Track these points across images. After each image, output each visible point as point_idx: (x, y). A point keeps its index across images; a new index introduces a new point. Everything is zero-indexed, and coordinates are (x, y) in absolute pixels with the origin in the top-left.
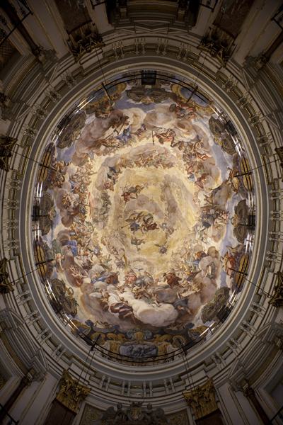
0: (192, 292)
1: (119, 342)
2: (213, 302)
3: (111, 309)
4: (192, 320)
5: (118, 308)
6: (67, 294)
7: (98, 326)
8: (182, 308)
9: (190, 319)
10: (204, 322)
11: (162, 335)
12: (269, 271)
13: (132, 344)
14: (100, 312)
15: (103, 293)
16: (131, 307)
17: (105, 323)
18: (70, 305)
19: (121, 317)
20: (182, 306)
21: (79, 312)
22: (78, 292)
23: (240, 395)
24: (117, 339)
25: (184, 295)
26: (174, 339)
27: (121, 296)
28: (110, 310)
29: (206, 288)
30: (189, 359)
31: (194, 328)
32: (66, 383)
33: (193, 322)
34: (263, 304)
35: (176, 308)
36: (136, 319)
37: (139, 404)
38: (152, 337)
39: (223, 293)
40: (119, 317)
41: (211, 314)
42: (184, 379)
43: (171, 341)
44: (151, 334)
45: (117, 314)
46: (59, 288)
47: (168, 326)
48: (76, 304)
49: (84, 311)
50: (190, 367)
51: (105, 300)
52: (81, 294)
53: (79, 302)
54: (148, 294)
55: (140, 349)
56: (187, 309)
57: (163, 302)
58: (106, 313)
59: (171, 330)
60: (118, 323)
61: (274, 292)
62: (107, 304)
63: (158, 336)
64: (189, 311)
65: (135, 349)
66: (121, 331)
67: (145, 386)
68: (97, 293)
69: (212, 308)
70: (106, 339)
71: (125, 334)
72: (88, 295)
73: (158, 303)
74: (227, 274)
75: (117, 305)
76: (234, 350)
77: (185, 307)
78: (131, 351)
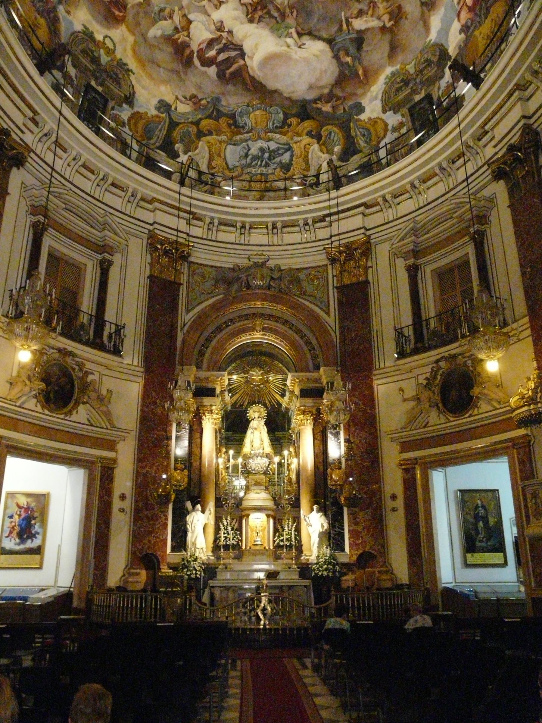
0: (374, 23)
1: (224, 138)
2: (411, 68)
3: (200, 58)
4: (364, 94)
5: (212, 53)
6: (104, 59)
7: (183, 108)
8: (349, 59)
9: (359, 91)
10: (384, 111)
11: (303, 120)
12: (520, 99)
13: (246, 141)
14: (178, 72)
15: (177, 18)
16: (239, 48)
17: (193, 97)
18: (117, 81)
19: (221, 75)
20: (348, 54)
21: (138, 89)
22: (124, 39)
23: (401, 264)
24: (219, 132)
25: (359, 24)
26: (324, 133)
27: (216, 15)
28: (196, 62)
29: (406, 25)
30: (340, 197)
31: (364, 117)
32: (157, 249)
33: (365, 102)
34: (485, 146)
35: (336, 57)
36: (253, 78)
37: (263, 264)
38: (284, 123)
39: (435, 59)
40: (218, 75)
41: (401, 96)
42: (331, 222)
43: (318, 137)
44: (281, 116)
45: (213, 70)
46: (84, 52)
47: (315, 101)
48: (129, 71)
49: (146, 82)
50: (340, 208)
51: (182, 37)
52: (131, 39)
53: (132, 64)
54: (278, 10)
55: (262, 150)
56: (357, 64)
57: (310, 34)
58: (189, 71)
59: (321, 109)
60: (217, 91)
61: (505, 149)
62: (186, 45)
63: (294, 121)
64: (360, 72)
65: (254, 151)
66: (225, 110)
67: (270, 227)
68: (163, 23)
69: (406, 82)
70: (200, 134)
71: (233, 116)
72: (144, 36)
73: (300, 35)
74: (458, 16)
75: (211, 43)
76: (414, 197)
77: (354, 58)
78: (246, 155)
